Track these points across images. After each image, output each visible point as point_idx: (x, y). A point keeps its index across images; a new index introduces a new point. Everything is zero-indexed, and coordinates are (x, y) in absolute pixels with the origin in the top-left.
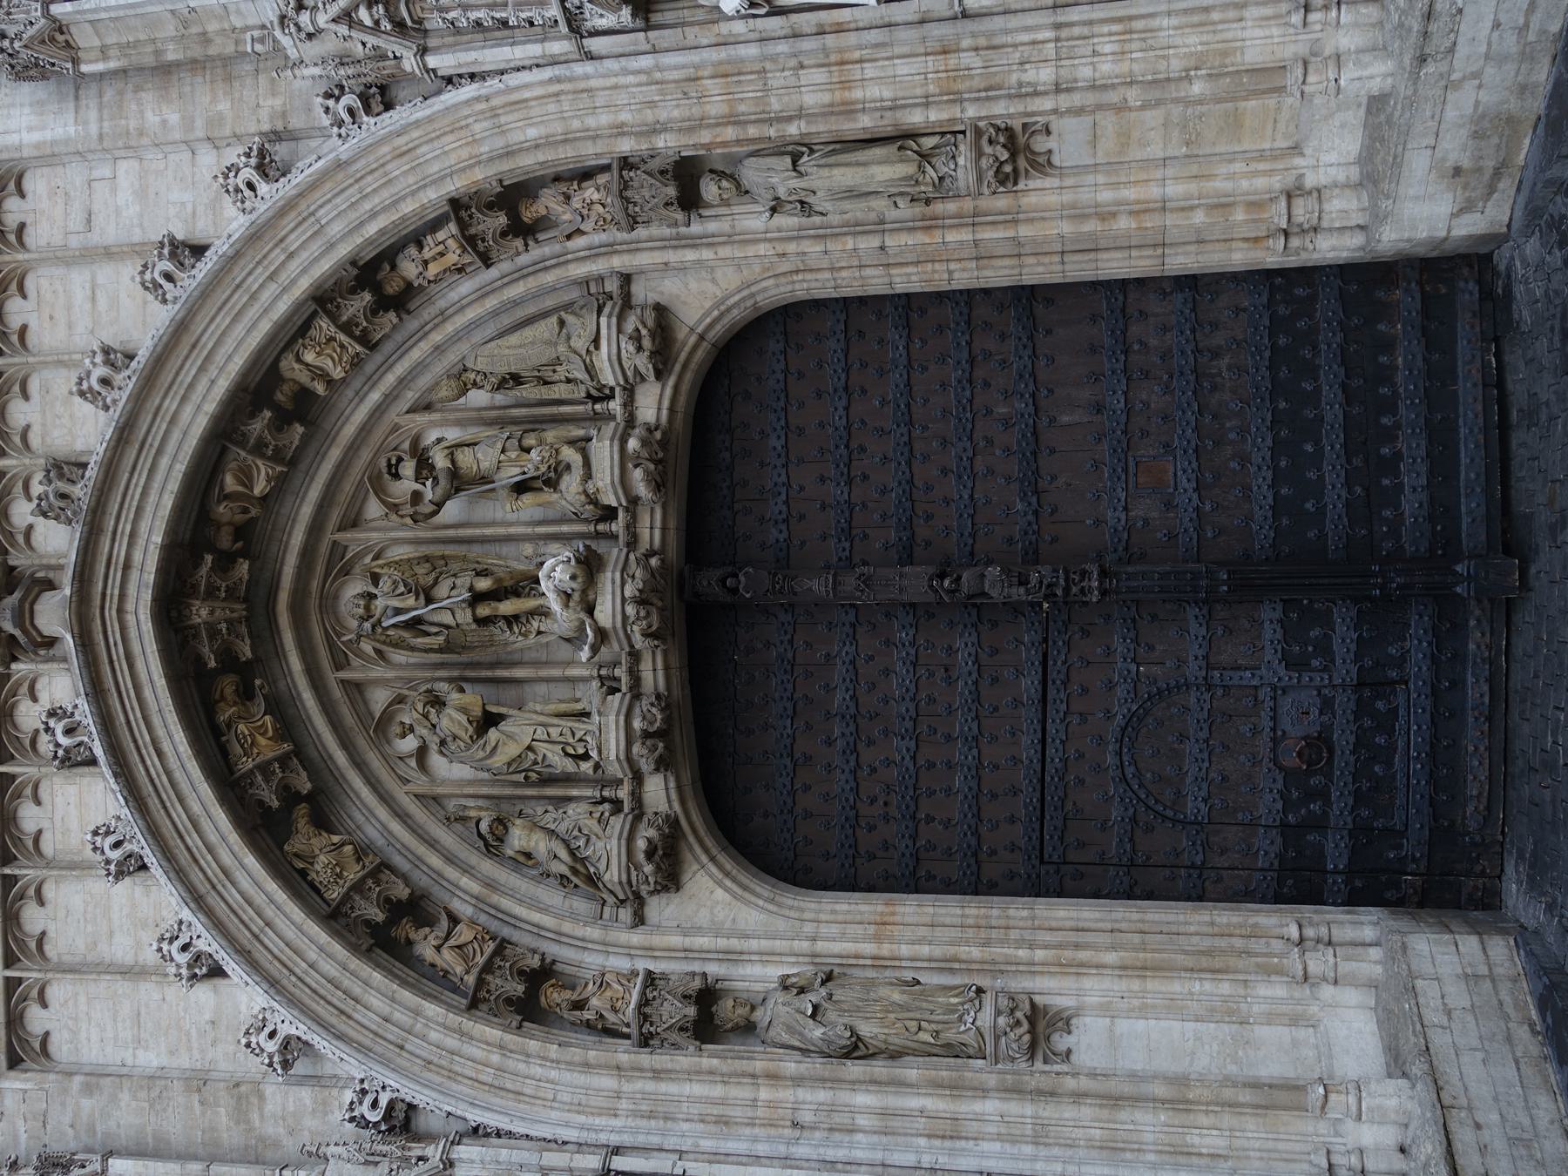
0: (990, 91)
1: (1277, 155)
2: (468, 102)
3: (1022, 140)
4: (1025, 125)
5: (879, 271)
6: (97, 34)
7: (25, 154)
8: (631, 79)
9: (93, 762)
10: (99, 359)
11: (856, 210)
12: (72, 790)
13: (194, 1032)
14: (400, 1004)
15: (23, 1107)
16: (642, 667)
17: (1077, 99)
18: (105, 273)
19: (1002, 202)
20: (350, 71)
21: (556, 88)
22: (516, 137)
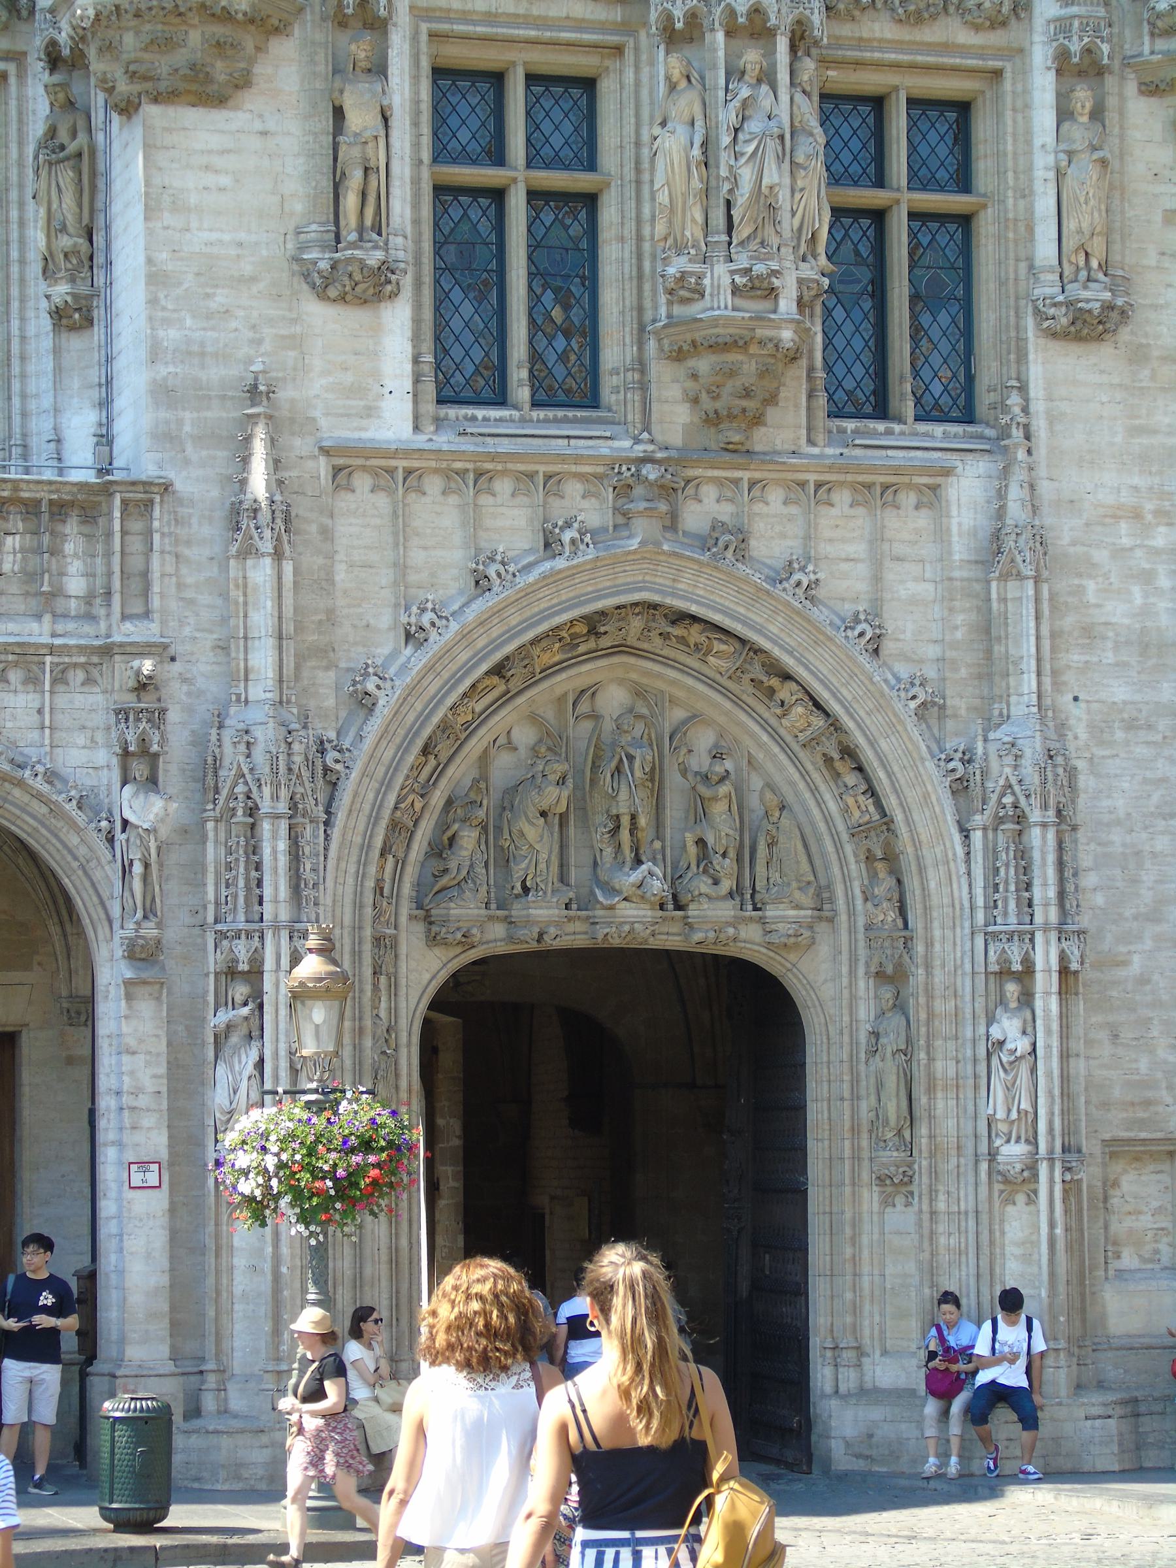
0: (934, 1173)
1: (883, 1339)
2: (953, 848)
3: (904, 1189)
4: (912, 1193)
5: (826, 1095)
6: (1014, 599)
7: (944, 520)
8: (959, 955)
9: (547, 545)
10: (812, 577)
11: (867, 1085)
12: (523, 523)
13: (360, 610)
14: (393, 775)
15: (307, 476)
16: (577, 923)
17: (926, 1224)
18: (863, 569)
19: (865, 1176)
20: (978, 777)
21: (957, 907)
22: (931, 873)
